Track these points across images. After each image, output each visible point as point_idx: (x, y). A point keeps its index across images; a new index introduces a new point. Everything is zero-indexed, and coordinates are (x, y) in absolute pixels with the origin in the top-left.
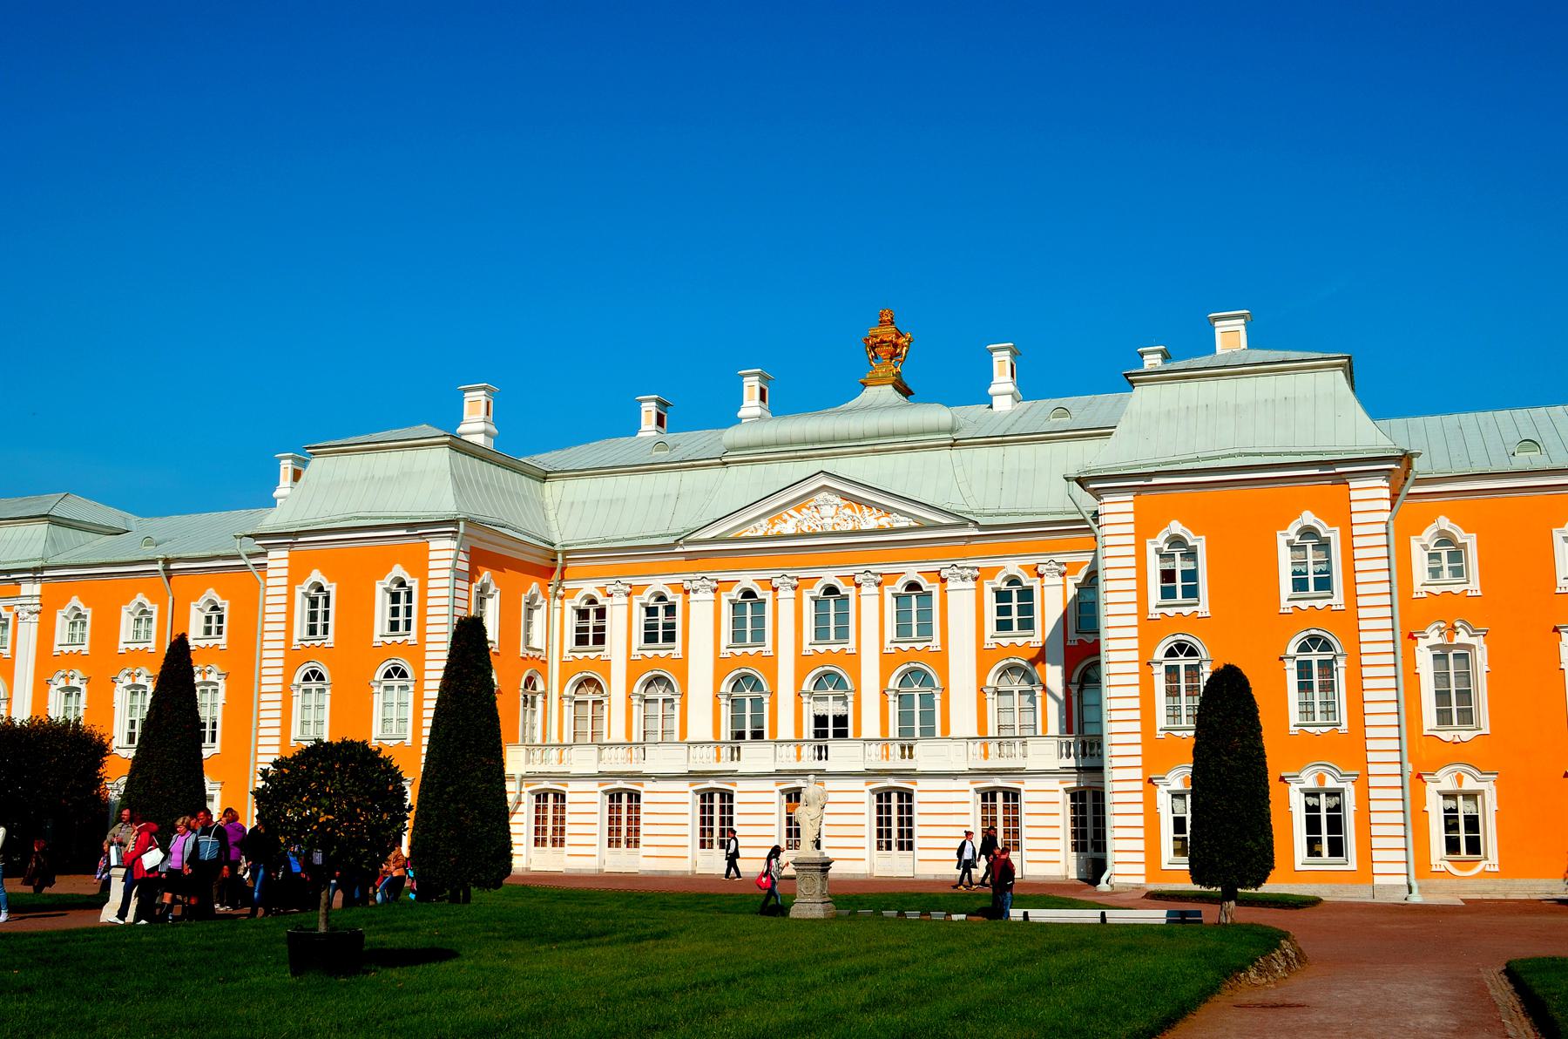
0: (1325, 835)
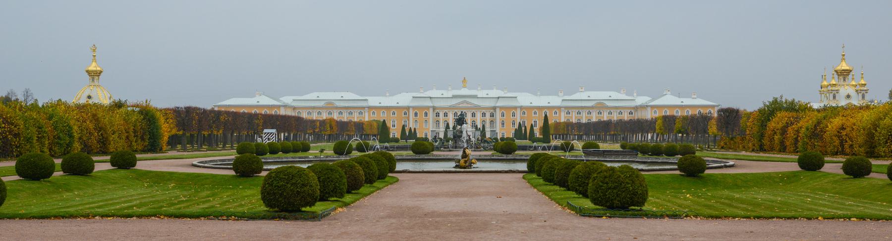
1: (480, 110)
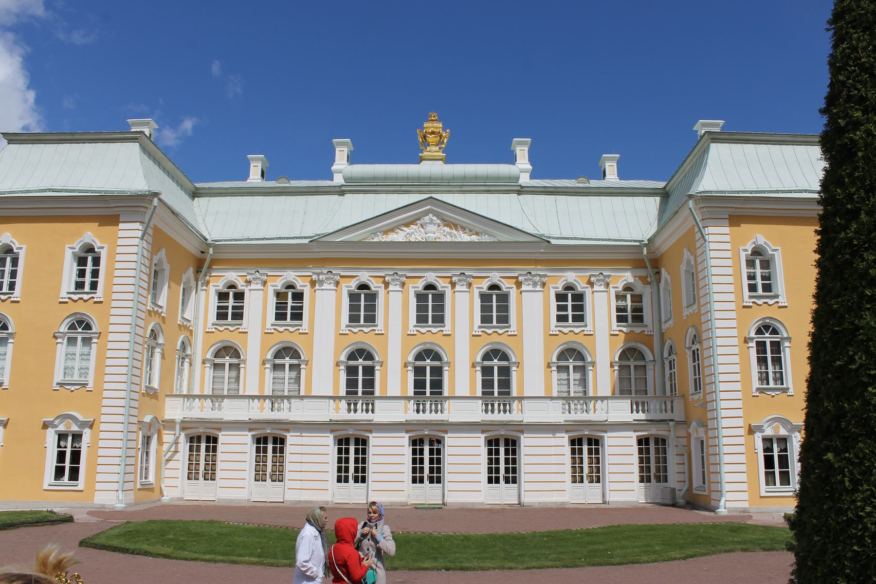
0: (777, 470)
1: (539, 270)
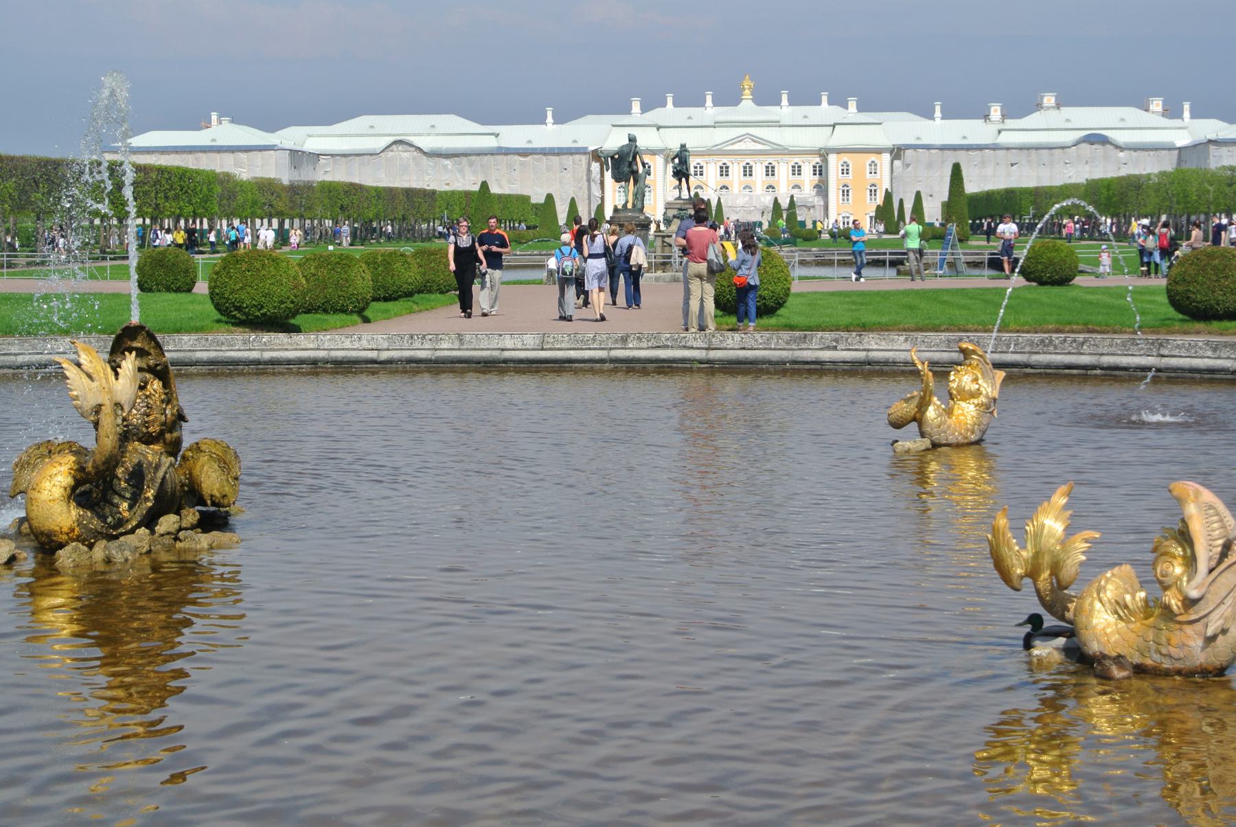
1: (786, 158)
